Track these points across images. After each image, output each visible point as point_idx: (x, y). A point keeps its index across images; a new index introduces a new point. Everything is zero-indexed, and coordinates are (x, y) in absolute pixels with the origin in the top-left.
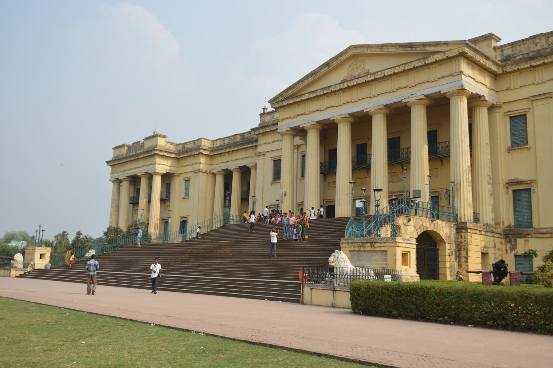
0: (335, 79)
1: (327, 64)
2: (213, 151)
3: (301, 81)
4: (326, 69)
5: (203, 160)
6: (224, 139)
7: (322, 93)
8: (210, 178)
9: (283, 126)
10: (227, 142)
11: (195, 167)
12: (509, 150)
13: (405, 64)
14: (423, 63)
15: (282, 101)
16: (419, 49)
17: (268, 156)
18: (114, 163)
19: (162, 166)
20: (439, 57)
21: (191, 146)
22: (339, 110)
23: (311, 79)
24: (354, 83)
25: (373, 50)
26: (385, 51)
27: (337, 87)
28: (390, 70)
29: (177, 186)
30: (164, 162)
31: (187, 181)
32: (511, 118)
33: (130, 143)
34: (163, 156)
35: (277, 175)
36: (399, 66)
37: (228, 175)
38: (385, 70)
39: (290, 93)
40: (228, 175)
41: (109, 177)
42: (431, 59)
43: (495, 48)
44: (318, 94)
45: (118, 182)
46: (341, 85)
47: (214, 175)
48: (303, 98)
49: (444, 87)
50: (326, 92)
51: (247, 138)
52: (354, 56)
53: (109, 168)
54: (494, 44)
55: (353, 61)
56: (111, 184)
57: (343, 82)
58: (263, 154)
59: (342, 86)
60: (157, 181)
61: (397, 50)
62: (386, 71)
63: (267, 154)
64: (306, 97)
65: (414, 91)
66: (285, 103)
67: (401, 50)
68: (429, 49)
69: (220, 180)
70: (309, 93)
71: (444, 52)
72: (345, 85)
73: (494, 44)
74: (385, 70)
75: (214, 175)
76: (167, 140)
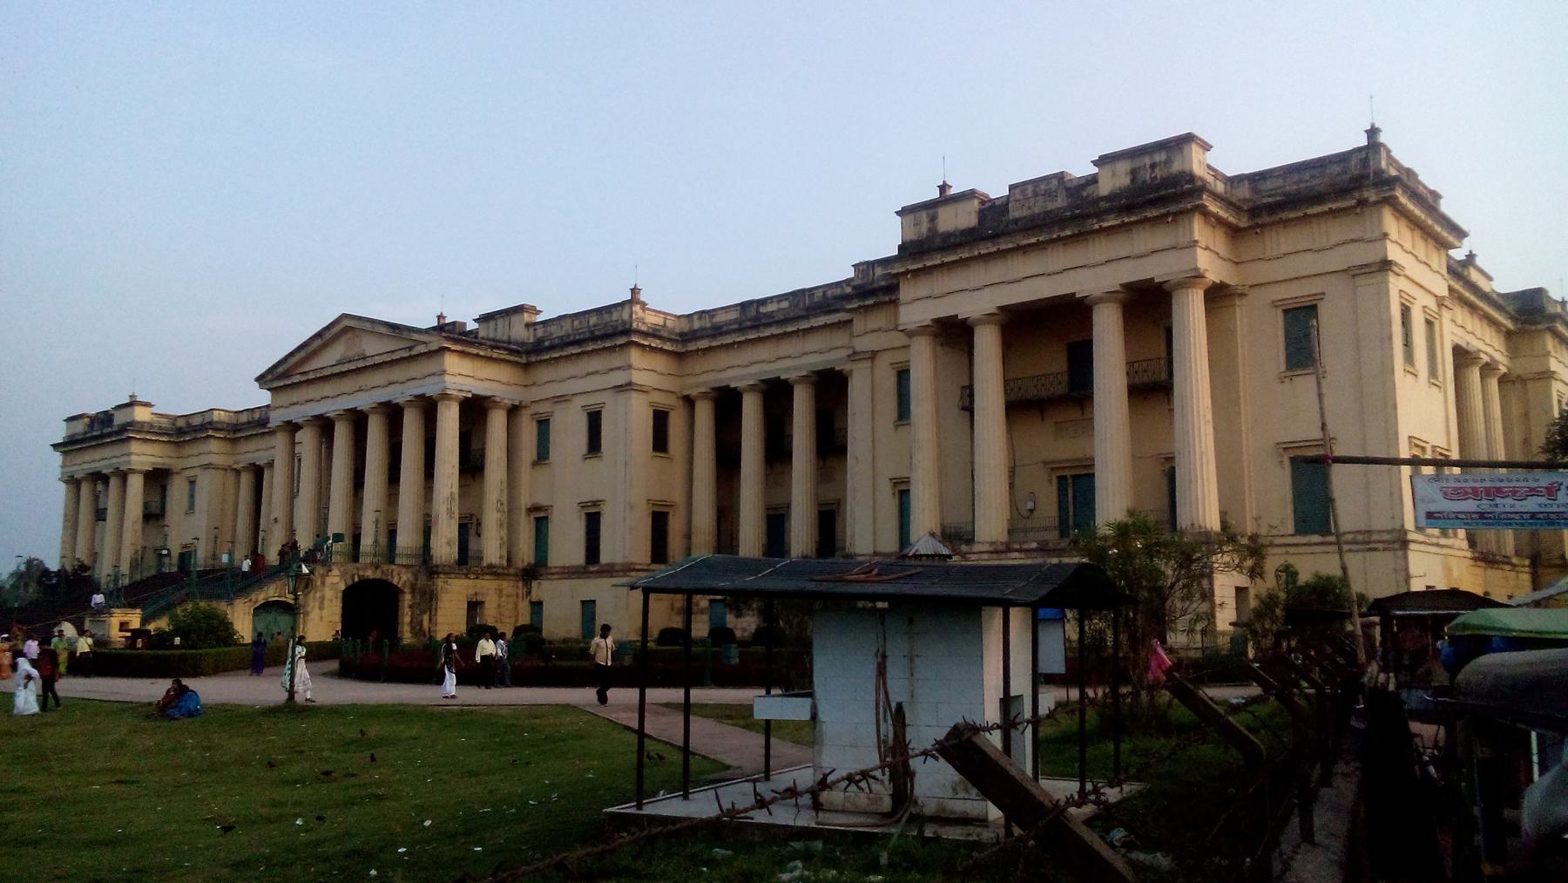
0: (330, 358)
1: (319, 335)
2: (236, 431)
3: (291, 354)
4: (318, 342)
6: (252, 410)
8: (231, 477)
9: (276, 418)
11: (205, 460)
12: (535, 464)
18: (69, 446)
19: (143, 456)
20: (422, 349)
21: (196, 421)
23: (302, 354)
29: (177, 490)
30: (148, 449)
31: (192, 483)
32: (540, 422)
33: (93, 412)
34: (145, 440)
39: (281, 370)
41: (58, 472)
43: (528, 325)
45: (73, 482)
47: (238, 472)
49: (430, 388)
52: (347, 329)
53: (57, 457)
54: (526, 317)
55: (349, 335)
56: (63, 485)
57: (339, 363)
60: (136, 484)
68: (416, 336)
69: (246, 479)
73: (526, 317)
76: (154, 410)
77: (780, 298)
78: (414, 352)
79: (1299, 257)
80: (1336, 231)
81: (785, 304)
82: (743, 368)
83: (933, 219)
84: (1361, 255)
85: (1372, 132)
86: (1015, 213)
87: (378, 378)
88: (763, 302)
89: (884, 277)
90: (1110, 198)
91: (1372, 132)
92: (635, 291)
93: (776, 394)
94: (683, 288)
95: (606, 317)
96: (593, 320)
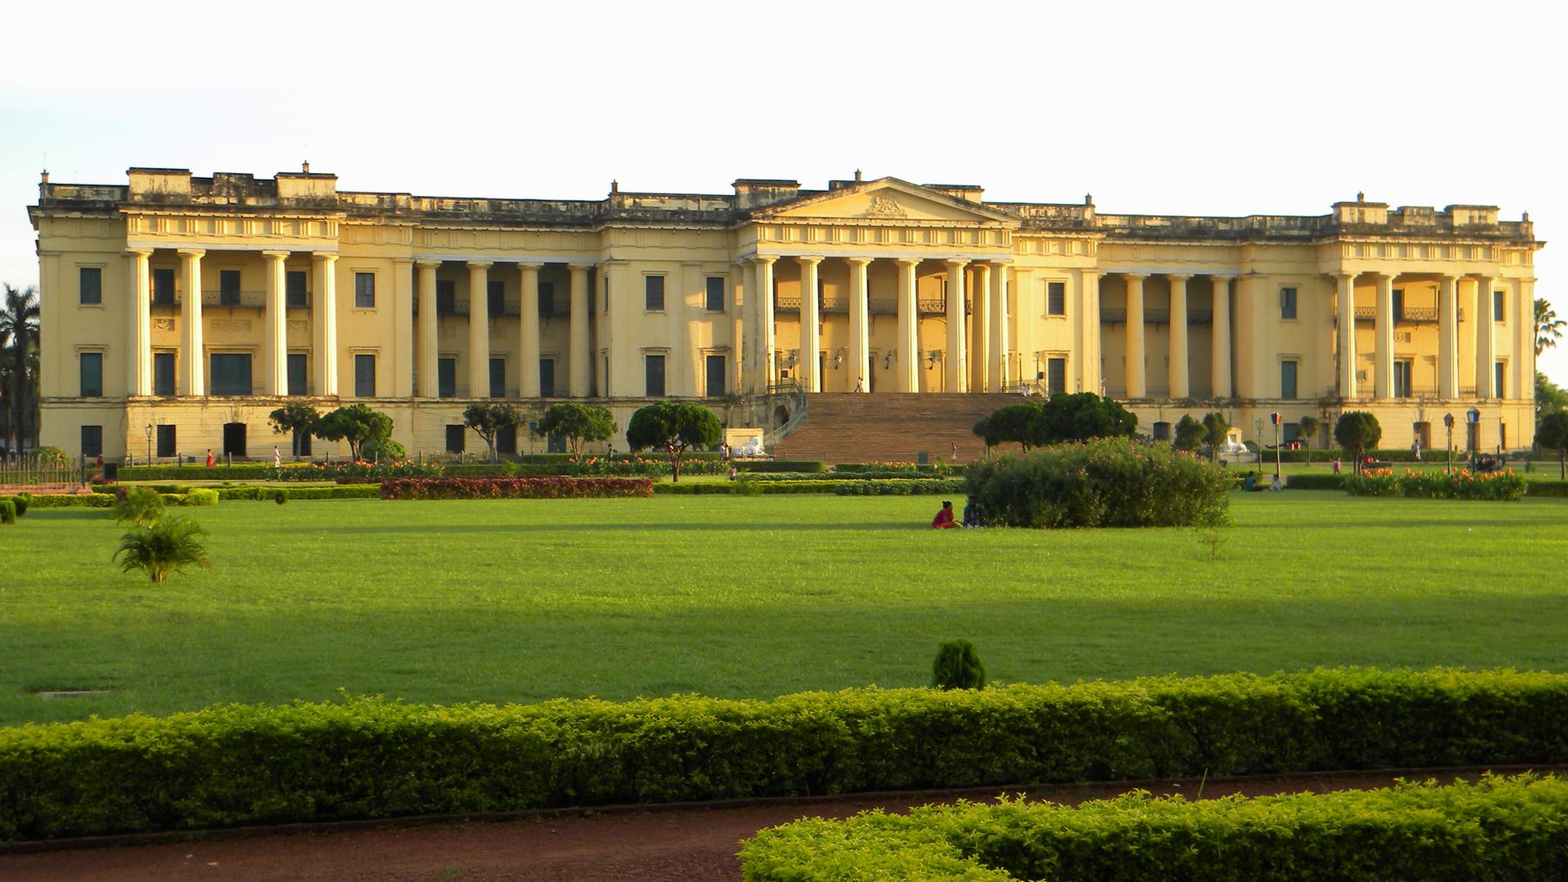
5: (409, 236)
6: (441, 199)
10: (449, 205)
22: (864, 251)
24: (891, 223)
27: (867, 223)
37: (452, 277)
40: (452, 277)
51: (510, 211)
52: (887, 189)
59: (873, 223)
63: (634, 265)
64: (817, 222)
65: (961, 252)
66: (779, 221)
72: (879, 223)
75: (417, 270)
77: (1163, 217)
79: (1502, 268)
80: (1515, 258)
81: (1167, 223)
82: (1137, 264)
83: (1362, 213)
84: (1521, 273)
85: (1525, 215)
86: (1407, 222)
88: (1150, 217)
89: (1272, 227)
90: (1460, 227)
91: (1525, 215)
92: (1088, 198)
93: (1158, 285)
94: (1114, 203)
95: (1065, 213)
96: (1052, 212)
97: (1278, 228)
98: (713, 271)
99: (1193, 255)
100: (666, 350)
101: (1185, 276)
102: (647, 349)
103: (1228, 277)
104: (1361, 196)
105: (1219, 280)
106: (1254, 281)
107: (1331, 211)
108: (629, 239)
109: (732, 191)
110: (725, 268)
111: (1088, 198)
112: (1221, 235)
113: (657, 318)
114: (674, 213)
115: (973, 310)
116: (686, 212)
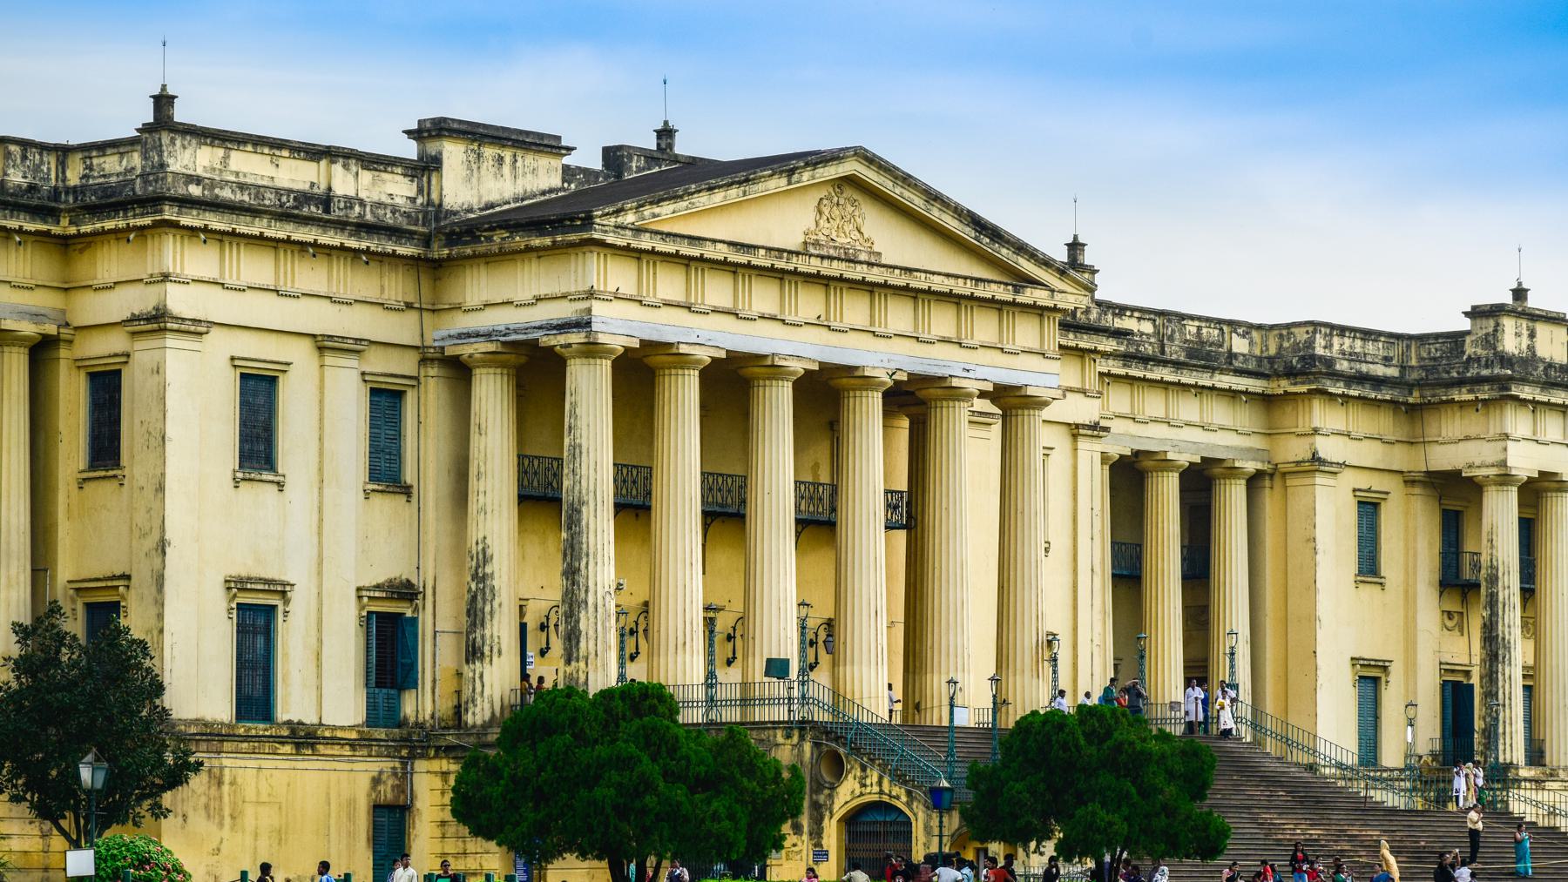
7: (767, 263)
13: (978, 280)
14: (1009, 297)
15: (638, 231)
16: (1004, 251)
17: (220, 346)
25: (906, 194)
26: (936, 214)
28: (946, 281)
35: (257, 449)
36: (966, 278)
38: (933, 273)
42: (1030, 296)
44: (755, 262)
46: (826, 263)
48: (710, 252)
50: (780, 264)
58: (196, 328)
61: (961, 227)
62: (937, 279)
64: (721, 252)
67: (967, 233)
70: (730, 244)
71: (1053, 291)
74: (933, 273)
78: (1020, 299)
87: (899, 316)
97: (1353, 357)
98: (378, 363)
99: (1188, 408)
100: (282, 590)
101: (1184, 458)
102: (236, 585)
103: (1251, 466)
104: (1520, 293)
105: (1232, 472)
106: (1320, 479)
107: (1465, 324)
108: (197, 260)
109: (410, 150)
110: (406, 364)
111: (1075, 247)
112: (1230, 363)
113: (260, 495)
114: (304, 198)
115: (911, 513)
116: (326, 200)
